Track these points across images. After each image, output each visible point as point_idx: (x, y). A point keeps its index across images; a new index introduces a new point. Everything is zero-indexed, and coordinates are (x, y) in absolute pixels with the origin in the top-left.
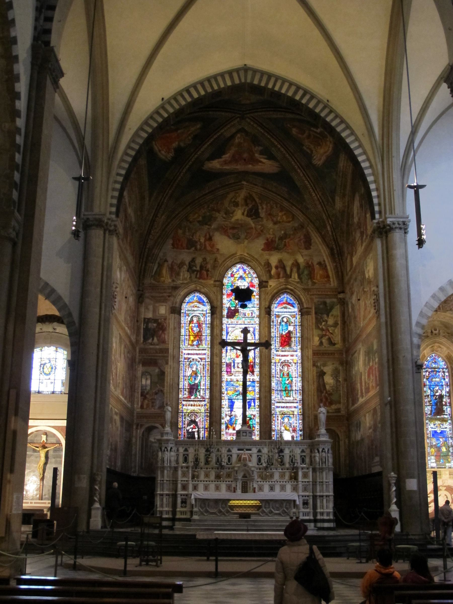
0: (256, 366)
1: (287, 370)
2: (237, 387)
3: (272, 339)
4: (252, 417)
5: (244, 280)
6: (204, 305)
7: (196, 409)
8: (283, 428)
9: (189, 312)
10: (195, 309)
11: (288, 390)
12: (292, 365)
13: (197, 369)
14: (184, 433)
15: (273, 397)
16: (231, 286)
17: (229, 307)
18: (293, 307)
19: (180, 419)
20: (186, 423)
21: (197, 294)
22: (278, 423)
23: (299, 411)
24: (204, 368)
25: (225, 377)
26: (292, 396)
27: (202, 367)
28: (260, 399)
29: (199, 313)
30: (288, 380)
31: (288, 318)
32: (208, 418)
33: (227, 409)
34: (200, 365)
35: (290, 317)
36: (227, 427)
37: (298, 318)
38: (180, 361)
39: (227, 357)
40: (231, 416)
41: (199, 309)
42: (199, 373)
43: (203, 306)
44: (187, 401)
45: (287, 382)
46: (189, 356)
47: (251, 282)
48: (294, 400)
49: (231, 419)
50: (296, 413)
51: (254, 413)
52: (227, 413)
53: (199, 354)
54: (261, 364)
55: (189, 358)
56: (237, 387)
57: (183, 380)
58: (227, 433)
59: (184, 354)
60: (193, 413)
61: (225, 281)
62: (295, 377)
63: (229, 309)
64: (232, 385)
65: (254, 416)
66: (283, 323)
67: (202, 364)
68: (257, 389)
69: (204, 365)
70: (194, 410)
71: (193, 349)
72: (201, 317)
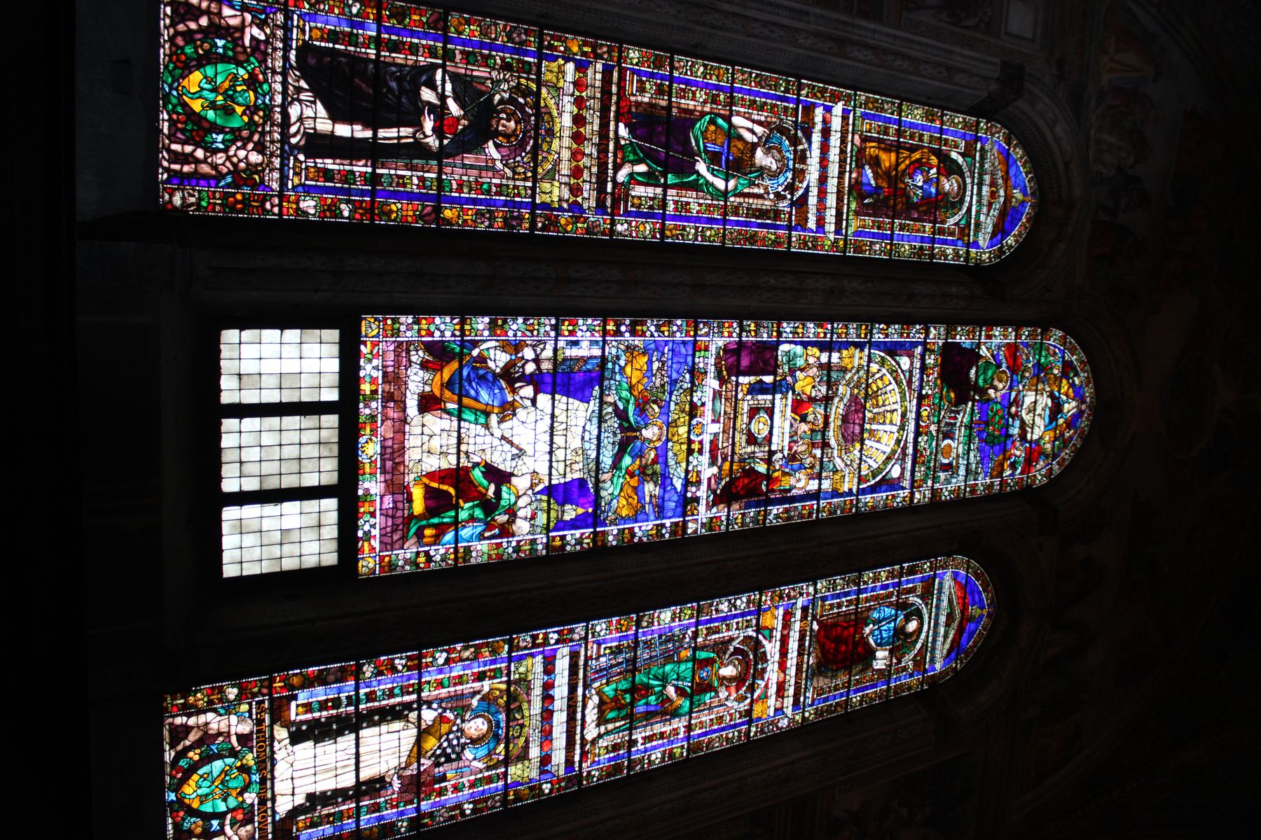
0: (752, 512)
1: (722, 679)
4: (503, 518)
7: (555, 145)
8: (429, 715)
10: (985, 190)
12: (741, 699)
13: (762, 170)
14: (413, 49)
15: (600, 626)
19: (499, 31)
20: (480, 72)
24: (762, 213)
25: (717, 340)
28: (599, 549)
29: (969, 209)
31: (916, 641)
33: (548, 353)
34: (778, 195)
35: (918, 646)
36: (438, 354)
38: (798, 78)
39: (799, 349)
41: (985, 210)
44: (606, 91)
46: (816, 138)
47: (1042, 453)
48: (583, 745)
50: (515, 771)
51: (522, 527)
52: (528, 353)
53: (822, 194)
56: (665, 410)
58: (403, 349)
59: (828, 110)
64: (673, 382)
65: (506, 531)
68: (643, 529)
69: (777, 214)
70: (551, 133)
71: (842, 162)
72: (957, 218)
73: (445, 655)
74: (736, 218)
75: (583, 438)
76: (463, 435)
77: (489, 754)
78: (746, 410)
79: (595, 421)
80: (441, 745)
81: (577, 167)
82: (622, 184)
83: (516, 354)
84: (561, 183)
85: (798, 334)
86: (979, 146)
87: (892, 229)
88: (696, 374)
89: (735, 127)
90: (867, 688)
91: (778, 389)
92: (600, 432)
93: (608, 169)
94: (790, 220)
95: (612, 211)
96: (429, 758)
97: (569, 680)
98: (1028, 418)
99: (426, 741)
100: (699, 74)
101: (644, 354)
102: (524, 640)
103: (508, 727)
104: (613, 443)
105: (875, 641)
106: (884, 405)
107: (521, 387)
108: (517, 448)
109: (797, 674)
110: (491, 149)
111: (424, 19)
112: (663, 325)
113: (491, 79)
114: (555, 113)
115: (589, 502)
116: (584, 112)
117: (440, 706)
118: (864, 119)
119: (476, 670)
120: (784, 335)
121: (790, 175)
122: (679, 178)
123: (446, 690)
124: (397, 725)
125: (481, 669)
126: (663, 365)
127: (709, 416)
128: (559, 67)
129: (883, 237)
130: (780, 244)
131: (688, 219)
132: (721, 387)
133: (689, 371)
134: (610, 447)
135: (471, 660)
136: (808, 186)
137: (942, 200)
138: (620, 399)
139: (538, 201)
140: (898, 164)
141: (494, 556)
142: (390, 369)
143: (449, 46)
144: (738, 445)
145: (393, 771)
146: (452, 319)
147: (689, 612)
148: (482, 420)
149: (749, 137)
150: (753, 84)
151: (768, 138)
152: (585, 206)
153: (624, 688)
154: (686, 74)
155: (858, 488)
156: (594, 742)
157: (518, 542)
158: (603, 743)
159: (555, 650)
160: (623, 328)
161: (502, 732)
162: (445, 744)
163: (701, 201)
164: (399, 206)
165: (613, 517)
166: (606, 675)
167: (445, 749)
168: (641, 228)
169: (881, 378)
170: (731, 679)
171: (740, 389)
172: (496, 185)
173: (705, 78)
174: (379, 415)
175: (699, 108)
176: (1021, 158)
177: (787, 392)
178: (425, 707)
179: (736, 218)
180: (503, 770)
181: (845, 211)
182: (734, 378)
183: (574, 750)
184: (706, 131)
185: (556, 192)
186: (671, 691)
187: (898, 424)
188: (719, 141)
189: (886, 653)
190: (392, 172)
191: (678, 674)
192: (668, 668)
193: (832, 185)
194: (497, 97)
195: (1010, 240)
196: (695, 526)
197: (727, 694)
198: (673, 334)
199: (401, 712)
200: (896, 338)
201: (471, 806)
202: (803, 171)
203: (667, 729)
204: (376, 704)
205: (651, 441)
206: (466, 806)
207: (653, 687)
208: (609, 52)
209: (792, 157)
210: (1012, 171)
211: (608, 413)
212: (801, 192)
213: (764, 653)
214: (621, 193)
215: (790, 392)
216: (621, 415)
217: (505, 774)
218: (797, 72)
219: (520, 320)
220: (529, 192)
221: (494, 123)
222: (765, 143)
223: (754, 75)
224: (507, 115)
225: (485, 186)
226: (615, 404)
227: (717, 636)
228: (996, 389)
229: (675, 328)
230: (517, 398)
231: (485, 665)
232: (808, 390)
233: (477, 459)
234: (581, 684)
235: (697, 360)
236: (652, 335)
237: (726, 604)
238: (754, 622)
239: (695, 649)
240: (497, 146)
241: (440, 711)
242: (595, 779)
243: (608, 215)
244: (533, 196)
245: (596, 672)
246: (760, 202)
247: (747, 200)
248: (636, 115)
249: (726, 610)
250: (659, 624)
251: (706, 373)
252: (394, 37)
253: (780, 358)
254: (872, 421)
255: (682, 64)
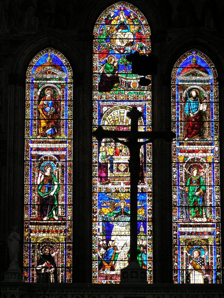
2: (117, 201)
3: (172, 124)
5: (127, 28)
6: (62, 70)
7: (51, 238)
8: (190, 267)
9: (38, 82)
10: (48, 76)
11: (199, 207)
12: (205, 167)
13: (51, 173)
14: (33, 275)
15: (174, 218)
16: (105, 39)
17: (103, 73)
18: (207, 73)
21: (52, 53)
22: (182, 259)
23: (217, 240)
24: (63, 172)
25: (98, 185)
26: (204, 216)
27: (60, 170)
28: (153, 220)
29: (55, 84)
30: (198, 190)
32: (71, 252)
33: (101, 237)
34: (57, 166)
35: (202, 89)
37: (214, 90)
39: (101, 154)
40: (108, 247)
42: (55, 179)
43: (61, 72)
44: (36, 224)
45: (197, 193)
46: (40, 153)
47: (138, 32)
48: (208, 222)
49: (107, 253)
50: (211, 243)
52: (101, 243)
54: (154, 164)
55: (40, 156)
56: (117, 201)
57: (29, 191)
59: (32, 149)
60: (47, 243)
61: (96, 31)
62: (210, 186)
63: (103, 75)
66: (191, 100)
67: (60, 165)
69: (62, 166)
70: (48, 239)
71: (46, 142)
73: (175, 263)
74: (65, 181)
75: (123, 226)
76: (121, 260)
77: (204, 250)
78: (118, 173)
79: (118, 223)
80: (199, 264)
81: (55, 231)
82: (58, 218)
83: (101, 246)
84: (60, 236)
85: (96, 155)
86: (34, 82)
87: (64, 119)
88: (108, 191)
89: (40, 183)
90: (212, 113)
91: (112, 162)
92: (121, 221)
93: (55, 223)
94: (64, 161)
95: (65, 221)
96: (202, 267)
97: (188, 227)
98: (125, 42)
99: (197, 268)
100: (28, 196)
101: (101, 209)
102: (175, 241)
103: (198, 245)
104: (125, 217)
105: (196, 111)
106: (118, 118)
107: (109, 245)
108: (124, 245)
109: (201, 145)
110: (53, 255)
111: (26, 272)
112: (94, 203)
113: (37, 255)
114: (43, 238)
115: (140, 223)
116: (42, 230)
117: (188, 264)
118: (33, 135)
119: (180, 255)
120: (96, 161)
121: (52, 162)
122: (55, 200)
123: (184, 263)
124: (191, 275)
125: (180, 253)
126: (104, 202)
127: (119, 186)
128: (32, 237)
129: (66, 123)
130: (71, 165)
131: (66, 197)
132: (111, 183)
133: (106, 194)
134: (126, 218)
135: (177, 256)
136: (55, 155)
137: (53, 98)
138: (113, 216)
139: (64, 242)
140: (45, 119)
141: (151, 250)
142: (104, 278)
143: (31, 266)
144: (127, 175)
145: (203, 276)
146: (93, 263)
147: (174, 189)
148: (117, 255)
149: (42, 178)
150: (28, 177)
151: (42, 171)
152: (65, 229)
153: (193, 210)
154: (28, 200)
155: (144, 126)
156: (207, 219)
157: (148, 244)
158: (208, 216)
159: (179, 232)
160: (95, 216)
161: (199, 247)
162: (199, 263)
163: (61, 193)
164: (68, 277)
165: (144, 216)
166: (188, 216)
167: (200, 263)
168: (69, 212)
169: (109, 119)
170: (198, 172)
171: (112, 176)
172: (61, 253)
173: (29, 194)
174: (115, 281)
175: (37, 195)
176: (36, 59)
177: (113, 158)
178: (188, 268)
179: (65, 181)
180: (210, 246)
181: (60, 140)
182: (108, 178)
183: (209, 225)
184: (43, 193)
185: (62, 237)
186: (197, 193)
187: (124, 110)
188: (45, 188)
189: (201, 105)
190: (60, 279)
191: (193, 191)
192: (190, 195)
193: (53, 146)
194: (41, 254)
195: (64, 61)
196: (149, 189)
197: (202, 172)
198: (96, 200)
199: (188, 274)
200: (97, 114)
201: (218, 255)
202: (50, 157)
203: (209, 194)
204: (185, 281)
205: (125, 205)
206: (217, 257)
207: (195, 200)
208: (27, 224)
209: (46, 162)
210: (41, 63)
211: (117, 219)
212: (56, 158)
213: (192, 159)
214: (61, 218)
215: (113, 157)
216: (118, 215)
217: (211, 245)
218: (22, 162)
219: (93, 245)
220: (62, 244)
221: (47, 254)
222: (44, 171)
223: (26, 177)
224: (45, 251)
225: (62, 256)
226: (115, 217)
227: (183, 178)
228: (114, 62)
229: (95, 199)
230: (112, 245)
231: (180, 252)
232: (112, 150)
233: (127, 256)
234: (190, 224)
235: (103, 192)
236: (97, 206)
237: (174, 175)
238: (181, 164)
239: (186, 186)
240: (52, 253)
241: (190, 264)
242: (219, 218)
243: (66, 222)
244: (63, 243)
245: (187, 219)
246: (60, 173)
247: (60, 177)
248: (41, 215)
249: (176, 175)
250: (177, 199)
251: (107, 188)
252: (31, 280)
253: (103, 162)
254: (122, 122)
255: (26, 201)
